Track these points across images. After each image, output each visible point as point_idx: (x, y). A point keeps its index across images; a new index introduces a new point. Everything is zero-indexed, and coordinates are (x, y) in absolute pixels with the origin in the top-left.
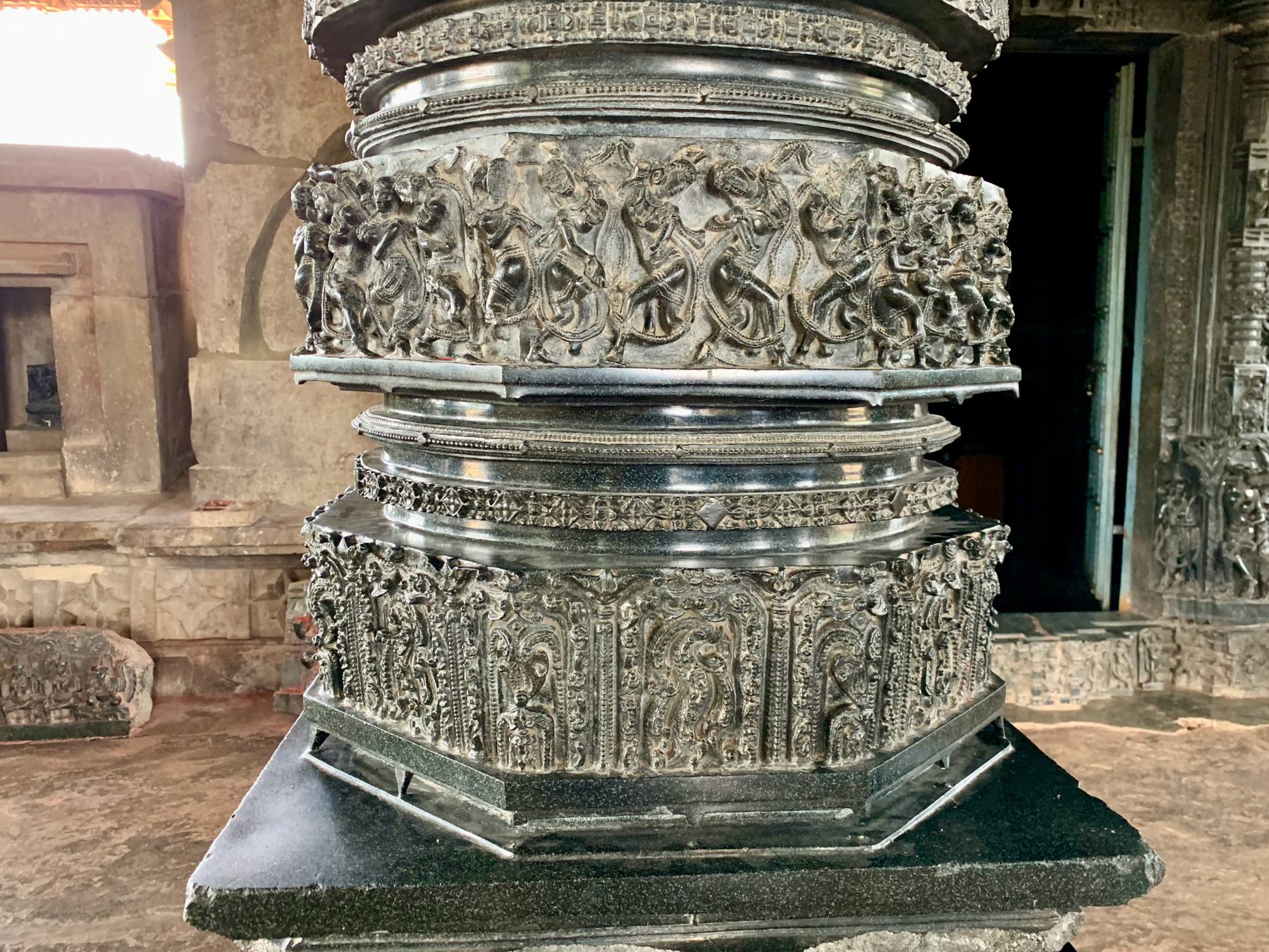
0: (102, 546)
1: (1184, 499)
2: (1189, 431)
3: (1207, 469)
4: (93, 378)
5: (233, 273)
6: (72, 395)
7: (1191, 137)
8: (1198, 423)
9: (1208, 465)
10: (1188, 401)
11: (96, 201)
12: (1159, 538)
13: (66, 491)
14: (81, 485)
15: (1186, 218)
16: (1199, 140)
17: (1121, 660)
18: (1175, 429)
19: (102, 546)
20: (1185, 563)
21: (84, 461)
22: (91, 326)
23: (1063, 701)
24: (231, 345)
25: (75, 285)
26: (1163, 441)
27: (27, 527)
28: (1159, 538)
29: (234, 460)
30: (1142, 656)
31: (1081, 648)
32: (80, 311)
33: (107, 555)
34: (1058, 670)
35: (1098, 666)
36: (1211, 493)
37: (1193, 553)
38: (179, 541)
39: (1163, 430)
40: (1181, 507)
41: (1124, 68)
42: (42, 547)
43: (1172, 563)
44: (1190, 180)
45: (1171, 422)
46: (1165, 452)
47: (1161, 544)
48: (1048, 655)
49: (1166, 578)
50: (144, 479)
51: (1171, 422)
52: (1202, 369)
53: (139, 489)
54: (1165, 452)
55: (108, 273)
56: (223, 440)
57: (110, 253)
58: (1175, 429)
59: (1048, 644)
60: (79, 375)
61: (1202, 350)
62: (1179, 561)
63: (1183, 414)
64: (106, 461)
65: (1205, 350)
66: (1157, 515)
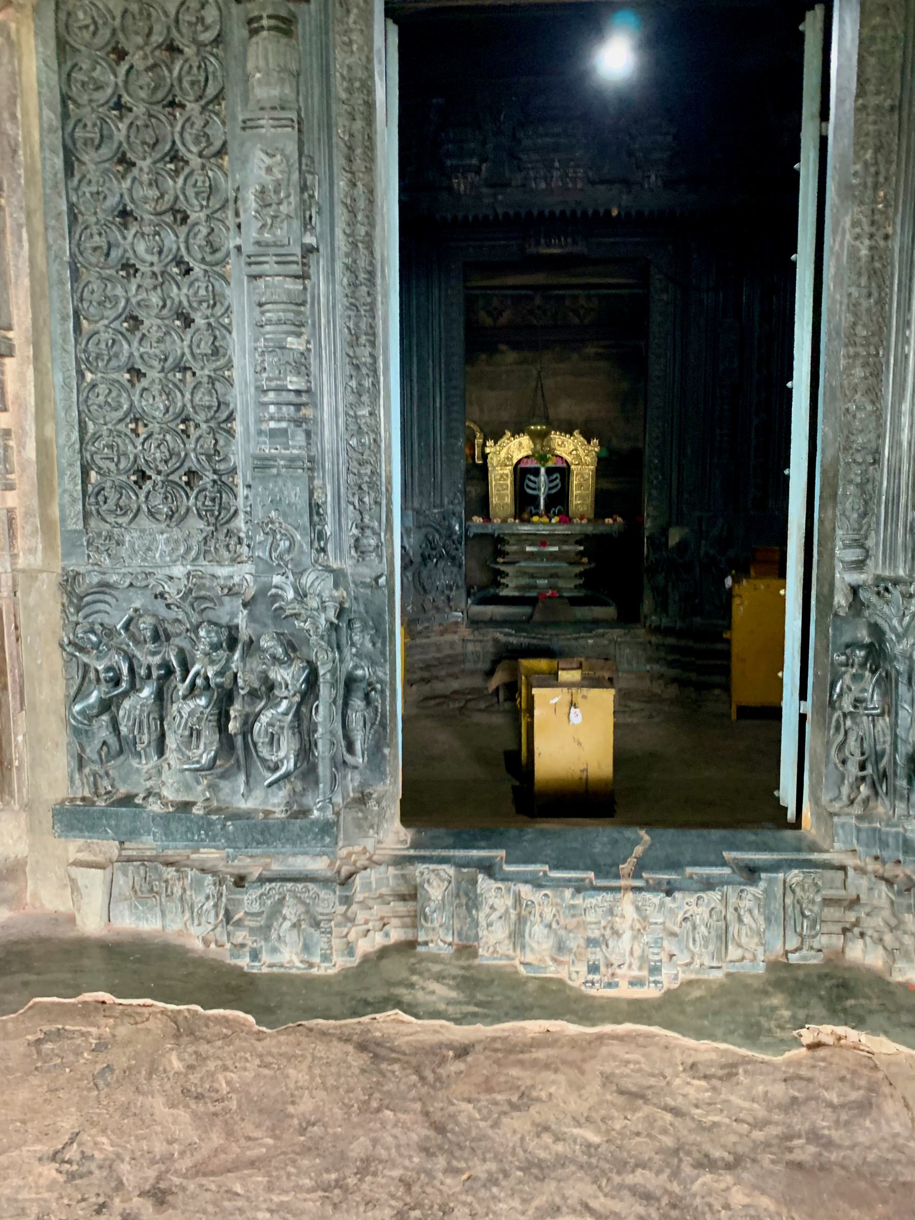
1: (867, 673)
2: (876, 568)
3: (893, 629)
7: (878, 107)
8: (890, 557)
9: (895, 622)
10: (878, 524)
12: (837, 729)
15: (871, 236)
16: (892, 109)
17: (747, 919)
18: (859, 565)
20: (869, 770)
23: (632, 984)
26: (838, 583)
28: (837, 729)
30: (790, 910)
31: (662, 905)
34: (627, 936)
35: (703, 929)
36: (901, 667)
37: (879, 756)
39: (839, 566)
40: (862, 685)
41: (809, 15)
43: (853, 769)
44: (877, 173)
45: (852, 555)
46: (841, 600)
47: (841, 737)
48: (611, 912)
49: (845, 790)
51: (852, 555)
52: (895, 473)
54: (841, 600)
58: (859, 565)
59: (609, 896)
61: (896, 444)
62: (862, 767)
63: (870, 543)
65: (900, 444)
66: (831, 696)
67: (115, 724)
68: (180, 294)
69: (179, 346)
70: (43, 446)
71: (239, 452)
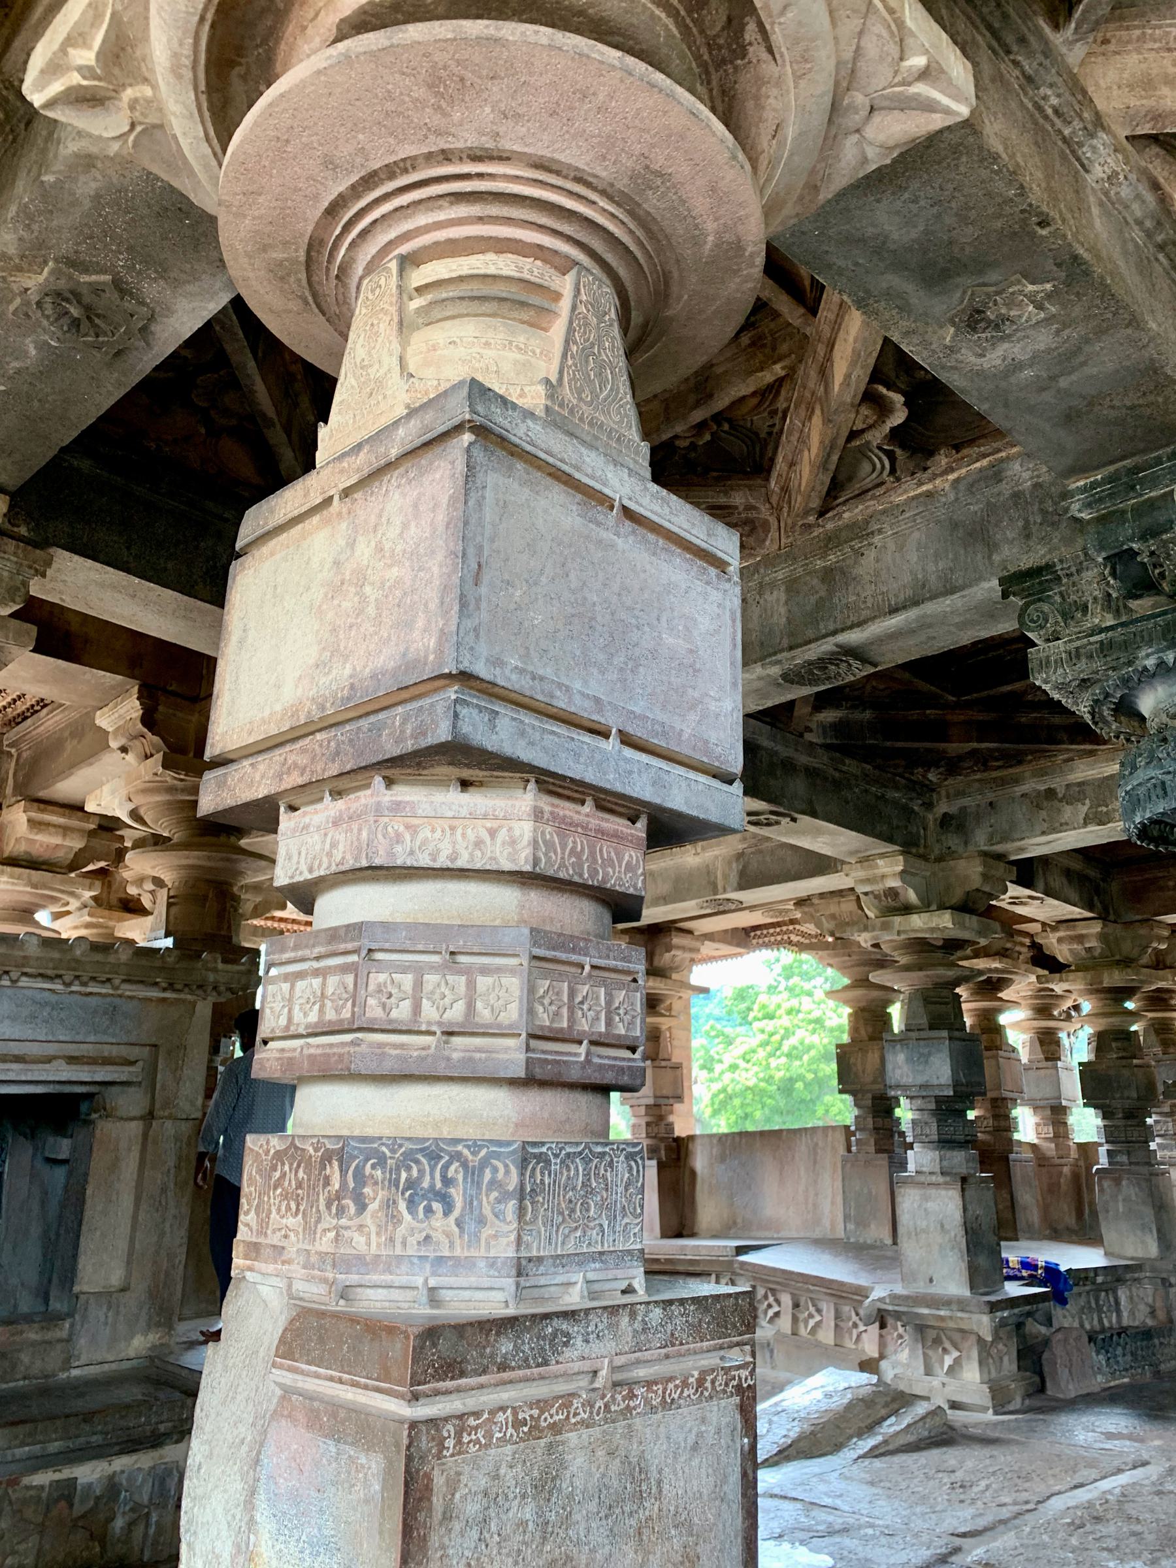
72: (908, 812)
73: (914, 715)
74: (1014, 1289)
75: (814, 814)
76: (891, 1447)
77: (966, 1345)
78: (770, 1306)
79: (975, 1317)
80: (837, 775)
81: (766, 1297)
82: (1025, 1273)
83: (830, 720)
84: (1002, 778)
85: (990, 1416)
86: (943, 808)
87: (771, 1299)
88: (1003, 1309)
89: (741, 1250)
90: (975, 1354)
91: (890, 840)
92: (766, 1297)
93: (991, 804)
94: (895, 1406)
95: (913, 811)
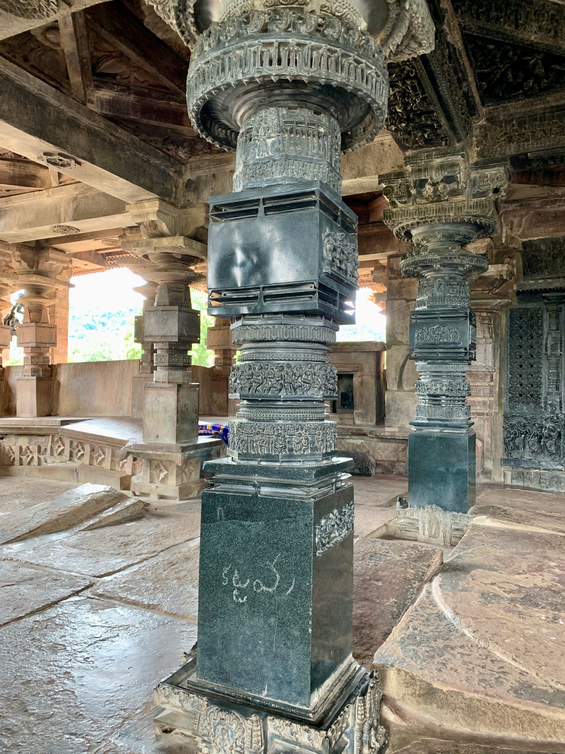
0: (365, 435)
4: (361, 396)
5: (396, 371)
6: (357, 400)
11: (365, 354)
13: (354, 423)
14: (358, 422)
19: (365, 435)
21: (358, 416)
22: (362, 383)
24: (395, 388)
25: (359, 374)
27: (350, 429)
29: (395, 416)
32: (359, 380)
33: (365, 437)
38: (382, 434)
42: (353, 434)
50: (372, 421)
53: (370, 424)
55: (366, 370)
56: (393, 411)
57: (367, 366)
60: (358, 395)
64: (363, 416)
67: (514, 443)
68: (532, 361)
69: (531, 370)
70: (500, 388)
71: (543, 391)
72: (165, 175)
73: (162, 104)
74: (203, 440)
75: (92, 161)
76: (103, 524)
77: (171, 468)
78: (79, 451)
79: (175, 454)
80: (113, 139)
81: (77, 446)
82: (213, 432)
83: (108, 97)
84: (220, 160)
85: (177, 502)
86: (188, 176)
87: (80, 447)
88: (190, 450)
89: (64, 423)
90: (175, 472)
91: (150, 189)
92: (77, 446)
93: (214, 175)
94: (115, 502)
95: (169, 175)
